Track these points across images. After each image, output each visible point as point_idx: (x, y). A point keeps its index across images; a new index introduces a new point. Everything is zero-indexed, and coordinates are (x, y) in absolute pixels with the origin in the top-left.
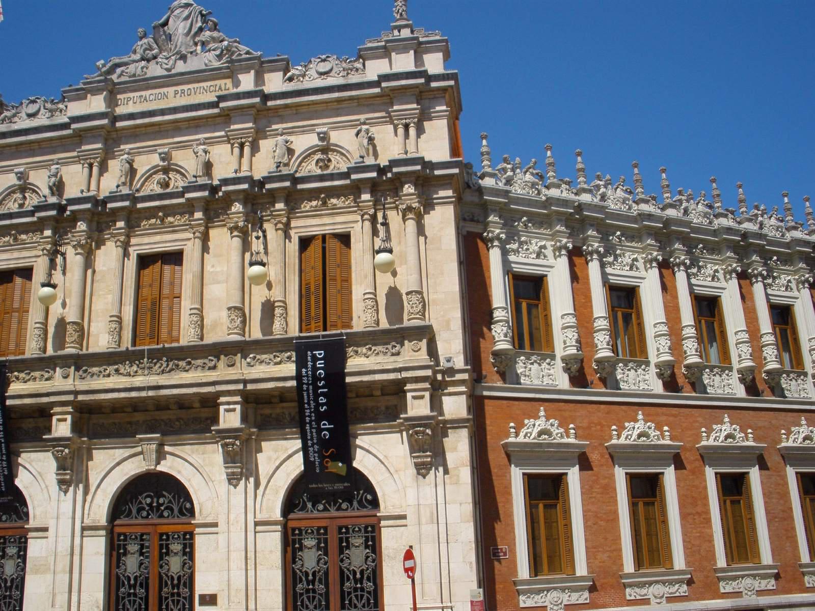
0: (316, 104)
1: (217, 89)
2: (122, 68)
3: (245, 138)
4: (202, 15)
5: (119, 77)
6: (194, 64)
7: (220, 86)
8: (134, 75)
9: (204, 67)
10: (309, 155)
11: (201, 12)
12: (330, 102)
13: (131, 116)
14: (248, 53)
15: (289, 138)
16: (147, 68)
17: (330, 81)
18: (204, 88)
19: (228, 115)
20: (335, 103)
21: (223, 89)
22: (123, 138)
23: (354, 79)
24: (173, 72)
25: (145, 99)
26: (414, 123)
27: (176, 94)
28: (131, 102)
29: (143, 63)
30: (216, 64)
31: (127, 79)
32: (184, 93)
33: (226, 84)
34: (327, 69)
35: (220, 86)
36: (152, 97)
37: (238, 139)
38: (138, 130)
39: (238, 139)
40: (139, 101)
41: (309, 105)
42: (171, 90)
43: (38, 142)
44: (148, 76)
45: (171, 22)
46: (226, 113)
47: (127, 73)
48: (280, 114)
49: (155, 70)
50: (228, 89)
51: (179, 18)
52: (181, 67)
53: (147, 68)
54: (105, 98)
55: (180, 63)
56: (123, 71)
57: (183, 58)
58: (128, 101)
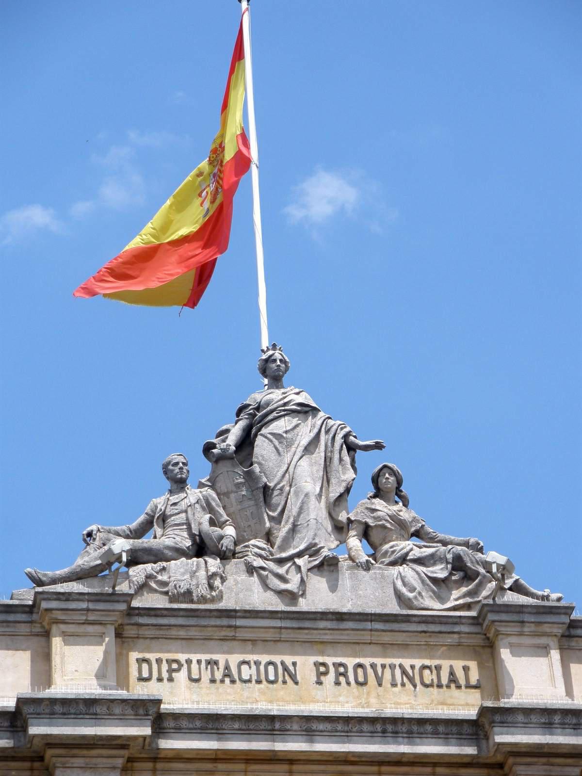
1: (445, 680)
2: (149, 568)
4: (351, 448)
5: (143, 587)
6: (364, 591)
7: (452, 673)
8: (187, 595)
9: (393, 608)
13: (211, 723)
16: (223, 580)
18: (404, 672)
19: (501, 766)
21: (462, 681)
24: (303, 605)
25: (228, 674)
27: (320, 674)
28: (181, 676)
29: (214, 564)
30: (433, 606)
32: (344, 675)
33: (466, 669)
35: (452, 673)
36: (247, 672)
40: (206, 676)
44: (227, 603)
45: (262, 447)
46: (499, 758)
47: (165, 584)
49: (242, 591)
51: (289, 445)
52: (319, 596)
53: (223, 580)
54: (66, 643)
55: (318, 584)
57: (328, 566)
58: (171, 671)
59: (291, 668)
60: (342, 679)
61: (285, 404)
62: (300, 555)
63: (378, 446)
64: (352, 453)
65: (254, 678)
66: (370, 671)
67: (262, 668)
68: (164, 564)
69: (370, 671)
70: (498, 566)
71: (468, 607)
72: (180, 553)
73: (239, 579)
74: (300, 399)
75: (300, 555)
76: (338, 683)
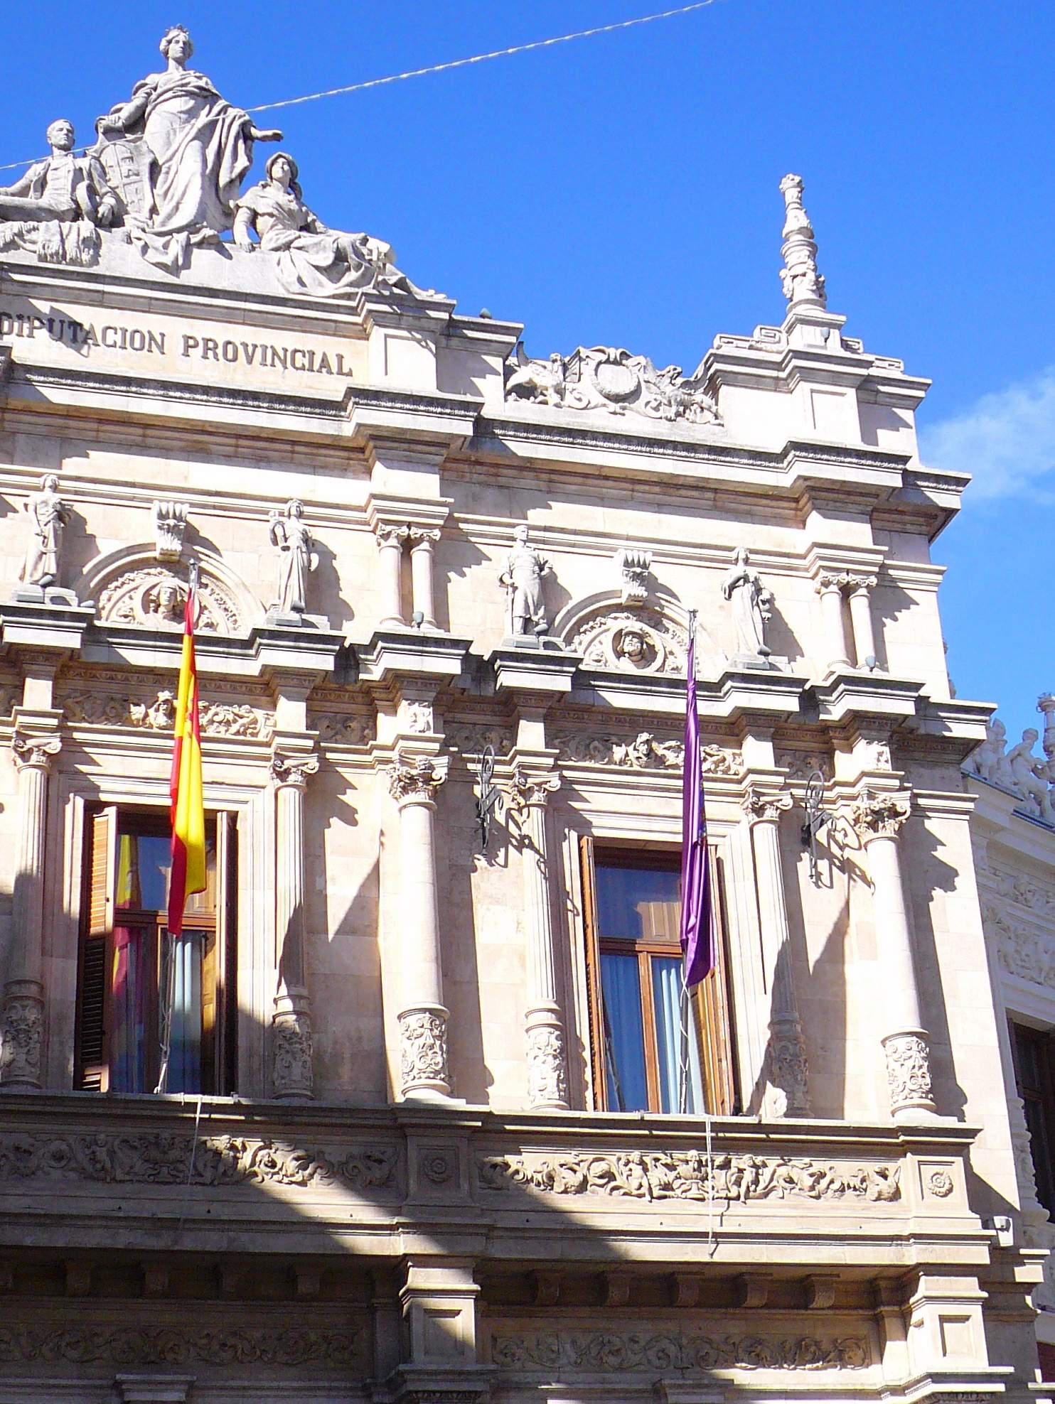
0: (606, 478)
1: (316, 367)
3: (419, 525)
10: (593, 616)
11: (244, 127)
12: (640, 482)
14: (400, 284)
15: (544, 556)
17: (635, 422)
20: (657, 489)
22: (21, 438)
23: (697, 429)
26: (868, 587)
27: (187, 347)
31: (34, 261)
34: (626, 387)
37: (399, 524)
38: (72, 423)
39: (399, 524)
41: (586, 476)
42: (174, 328)
43: (146, 426)
48: (502, 481)
50: (350, 374)
56: (20, 235)
59: (159, 339)
60: (210, 354)
61: (183, 85)
62: (179, 230)
63: (277, 137)
64: (249, 142)
65: (119, 344)
66: (241, 349)
67: (128, 335)
68: (36, 224)
69: (241, 349)
70: (379, 254)
71: (349, 296)
72: (52, 214)
73: (113, 248)
74: (202, 83)
75: (179, 230)
76: (205, 357)
